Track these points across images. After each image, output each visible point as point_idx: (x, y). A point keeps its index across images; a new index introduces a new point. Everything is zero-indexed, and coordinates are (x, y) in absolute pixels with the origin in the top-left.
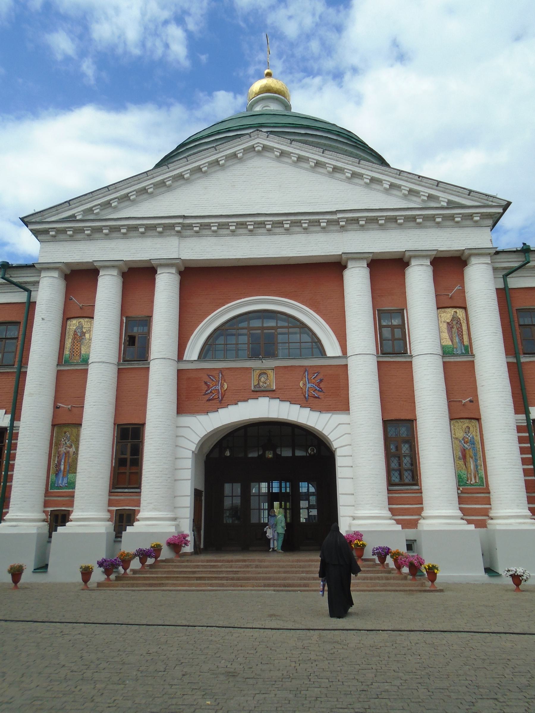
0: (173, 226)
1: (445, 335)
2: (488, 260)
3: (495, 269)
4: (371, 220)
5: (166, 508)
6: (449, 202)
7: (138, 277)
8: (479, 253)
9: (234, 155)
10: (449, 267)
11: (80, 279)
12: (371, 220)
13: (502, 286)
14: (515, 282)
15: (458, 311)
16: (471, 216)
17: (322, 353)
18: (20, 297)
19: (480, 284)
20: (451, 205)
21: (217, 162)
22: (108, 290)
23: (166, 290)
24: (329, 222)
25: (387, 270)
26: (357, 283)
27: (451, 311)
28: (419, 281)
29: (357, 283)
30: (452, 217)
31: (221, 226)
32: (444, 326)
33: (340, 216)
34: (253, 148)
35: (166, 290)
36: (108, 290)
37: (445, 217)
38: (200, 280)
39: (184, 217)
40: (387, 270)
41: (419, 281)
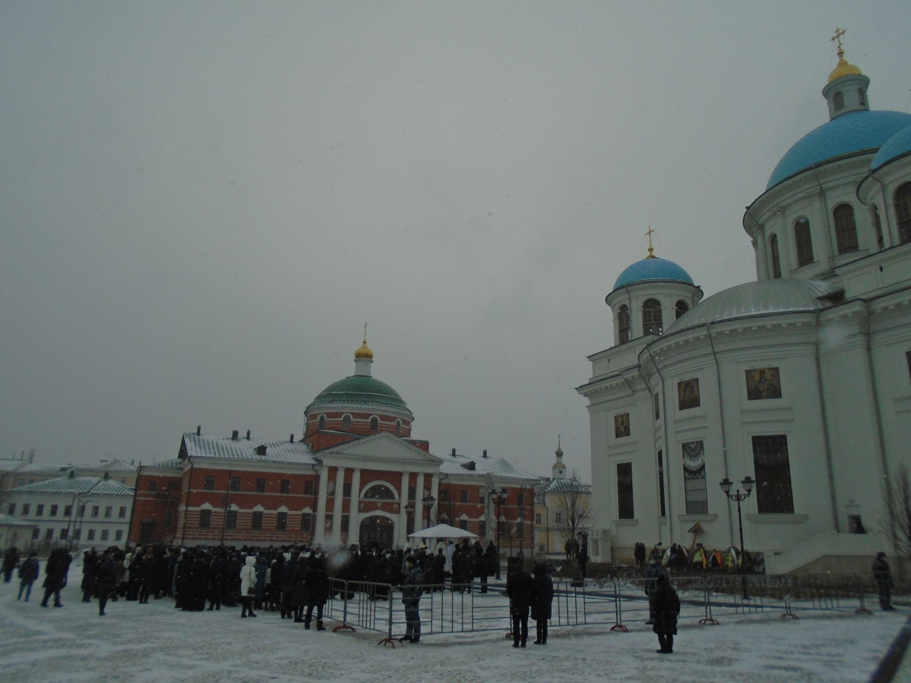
4: (413, 462)
5: (354, 538)
7: (349, 472)
10: (428, 477)
11: (333, 471)
12: (413, 462)
14: (443, 482)
17: (392, 497)
18: (314, 473)
22: (340, 477)
23: (356, 478)
25: (413, 476)
35: (356, 478)
36: (340, 477)
38: (367, 475)
40: (413, 476)
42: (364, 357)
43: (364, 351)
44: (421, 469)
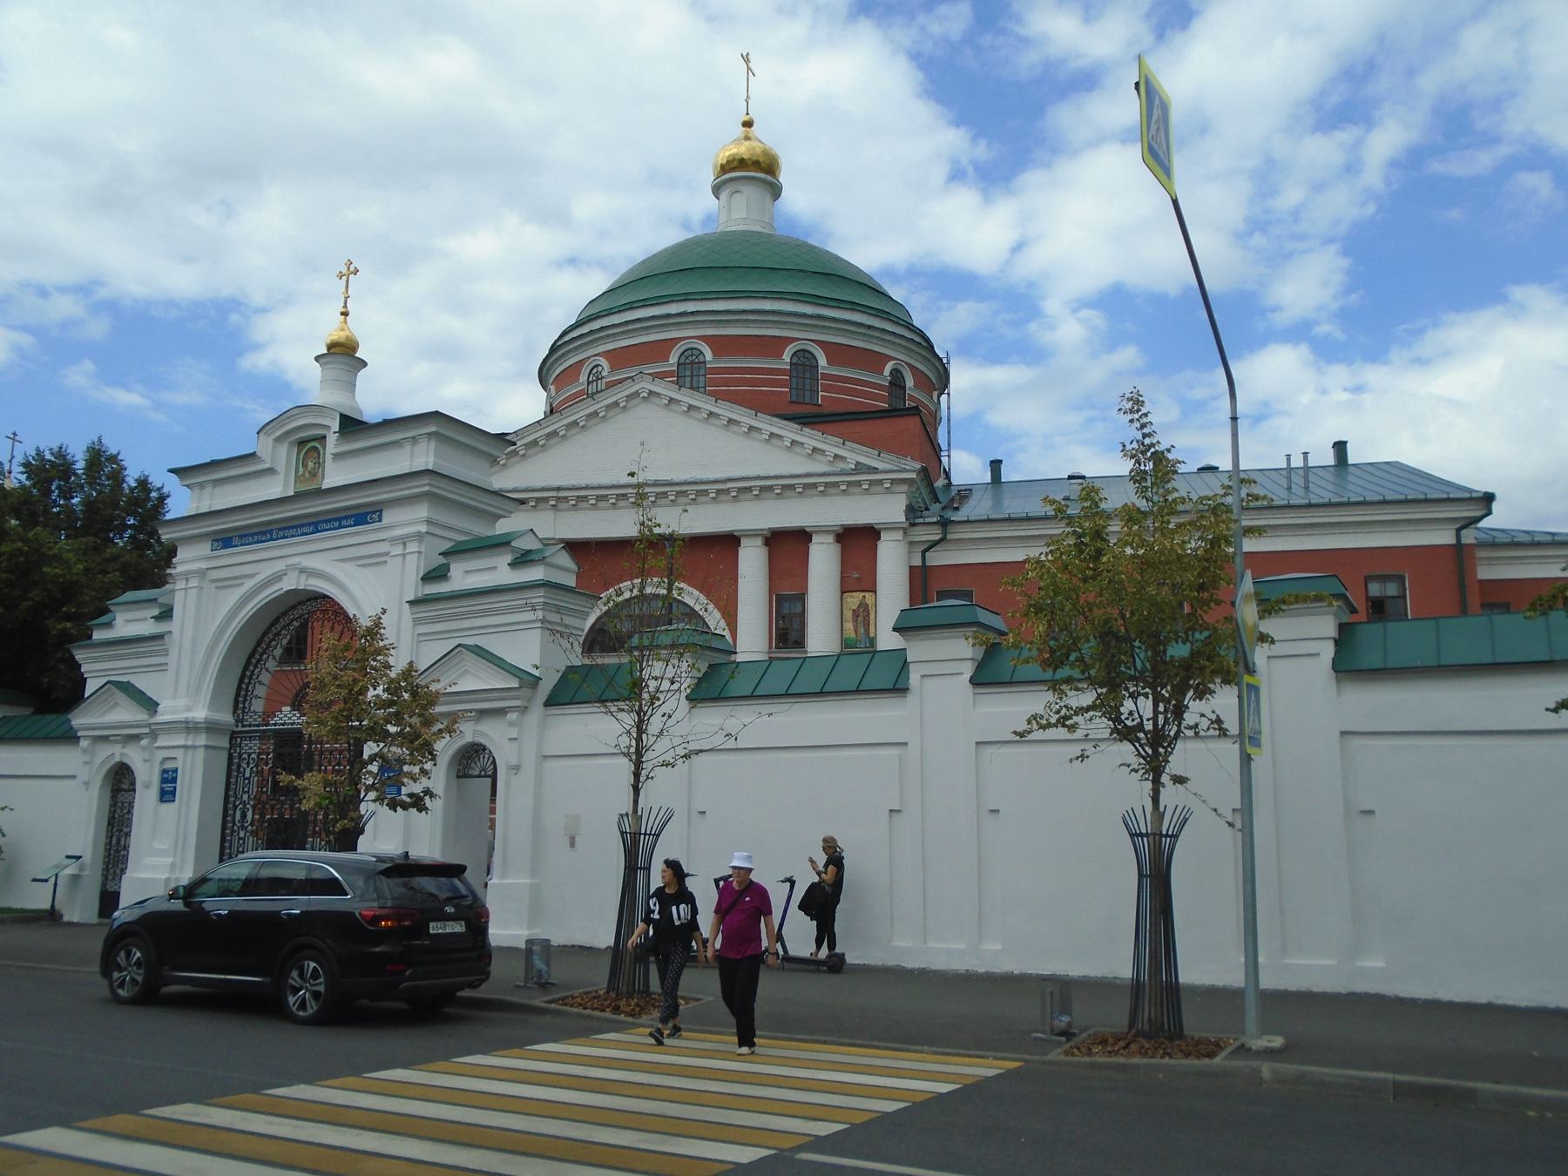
0: (546, 499)
1: (849, 626)
2: (899, 535)
3: (911, 543)
6: (858, 463)
8: (891, 528)
9: (616, 404)
10: (858, 542)
13: (917, 562)
14: (938, 558)
15: (867, 595)
16: (881, 482)
19: (892, 564)
20: (860, 468)
21: (596, 413)
24: (719, 492)
25: (787, 546)
26: (752, 562)
27: (859, 595)
28: (823, 561)
29: (752, 562)
30: (858, 484)
31: (600, 498)
32: (848, 614)
33: (729, 485)
34: (636, 394)
37: (849, 484)
39: (559, 489)
40: (787, 546)
41: (823, 561)
42: (753, 171)
43: (743, 150)
44: (824, 513)
